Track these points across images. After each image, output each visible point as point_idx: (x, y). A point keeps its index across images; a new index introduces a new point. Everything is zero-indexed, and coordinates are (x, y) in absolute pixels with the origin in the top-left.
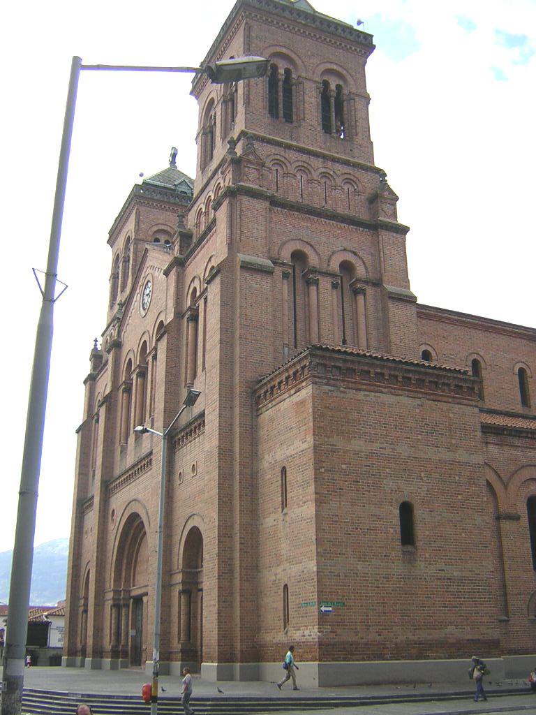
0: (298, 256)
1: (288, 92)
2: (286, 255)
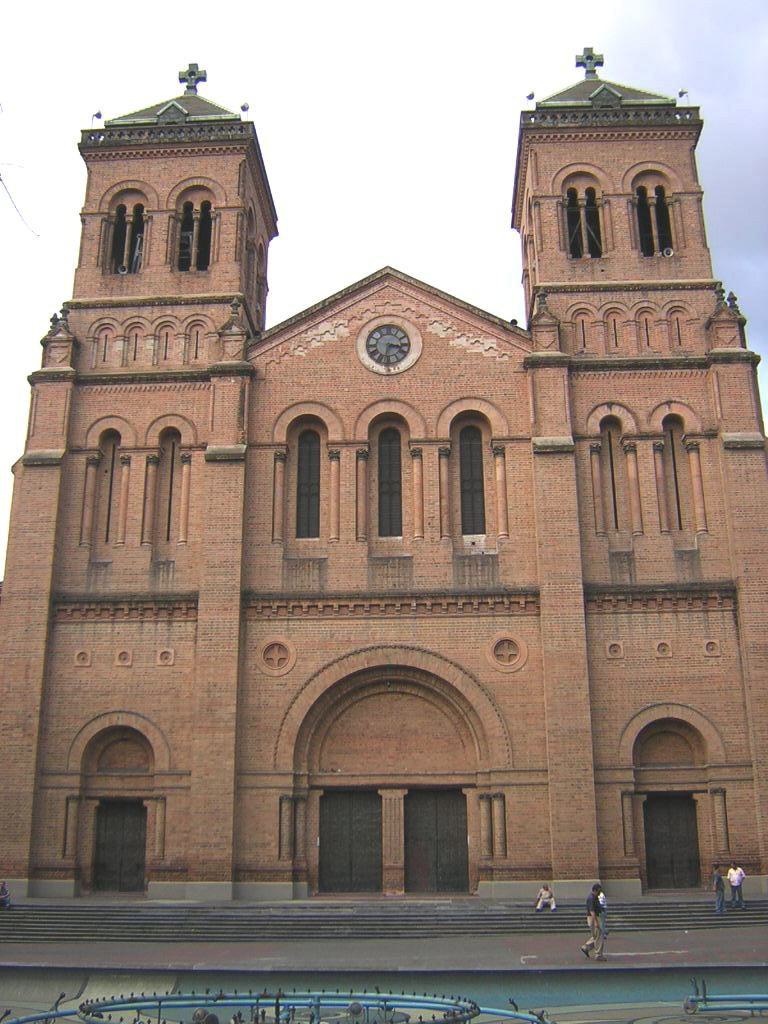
0: (611, 423)
1: (593, 219)
2: (593, 426)
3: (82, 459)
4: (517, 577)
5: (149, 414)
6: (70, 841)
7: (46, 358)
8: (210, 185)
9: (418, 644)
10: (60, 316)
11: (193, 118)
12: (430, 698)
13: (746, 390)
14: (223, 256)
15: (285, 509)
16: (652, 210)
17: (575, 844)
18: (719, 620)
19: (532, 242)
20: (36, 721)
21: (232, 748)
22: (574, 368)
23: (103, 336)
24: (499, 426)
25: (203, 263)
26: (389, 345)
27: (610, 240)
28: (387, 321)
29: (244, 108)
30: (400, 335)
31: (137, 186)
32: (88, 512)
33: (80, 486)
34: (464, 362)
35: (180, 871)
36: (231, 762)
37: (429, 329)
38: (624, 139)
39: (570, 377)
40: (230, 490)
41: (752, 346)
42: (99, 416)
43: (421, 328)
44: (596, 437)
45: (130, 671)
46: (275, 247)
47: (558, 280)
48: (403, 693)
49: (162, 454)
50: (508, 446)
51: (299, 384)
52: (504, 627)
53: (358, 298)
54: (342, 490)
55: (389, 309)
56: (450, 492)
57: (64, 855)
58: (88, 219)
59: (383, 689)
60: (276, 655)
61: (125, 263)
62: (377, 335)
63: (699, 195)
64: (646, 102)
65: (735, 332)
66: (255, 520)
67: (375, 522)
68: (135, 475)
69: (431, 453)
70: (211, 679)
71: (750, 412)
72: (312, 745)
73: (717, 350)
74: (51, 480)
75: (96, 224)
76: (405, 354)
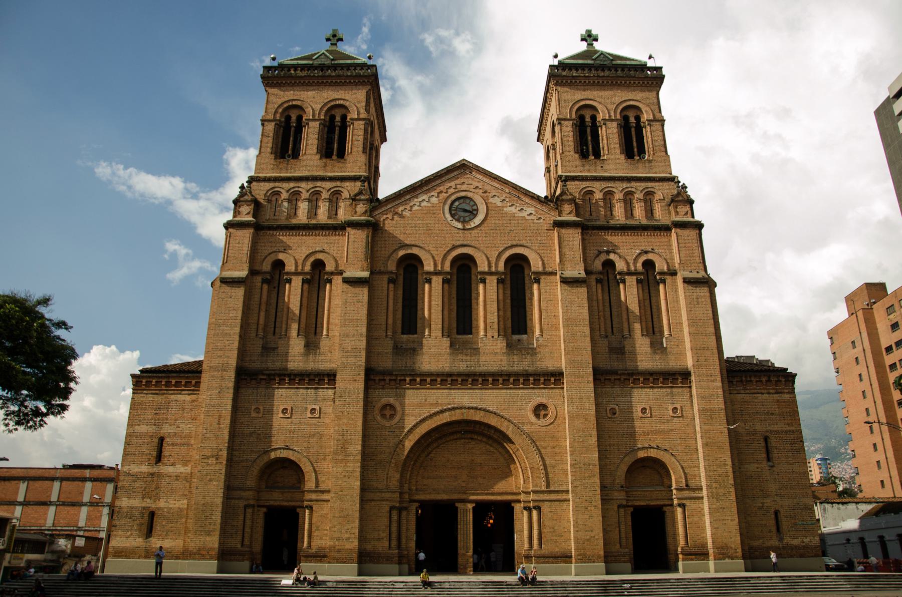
3: (259, 279)
4: (549, 364)
5: (305, 251)
6: (247, 535)
7: (236, 213)
8: (347, 104)
9: (483, 406)
10: (246, 185)
11: (336, 62)
12: (490, 442)
13: (695, 244)
14: (355, 150)
15: (394, 315)
16: (633, 130)
17: (588, 540)
18: (679, 393)
19: (554, 149)
20: (224, 453)
21: (359, 474)
22: (585, 228)
23: (274, 199)
24: (536, 264)
25: (341, 154)
26: (463, 210)
27: (606, 148)
28: (462, 194)
29: (370, 58)
30: (472, 203)
31: (299, 103)
32: (262, 314)
33: (256, 297)
34: (513, 222)
35: (320, 556)
36: (358, 483)
37: (491, 200)
38: (614, 85)
39: (582, 234)
40: (358, 301)
41: (697, 218)
42: (271, 251)
43: (486, 200)
44: (600, 273)
45: (290, 420)
46: (384, 149)
47: (574, 171)
48: (472, 439)
49: (312, 277)
50: (542, 277)
51: (405, 234)
52: (539, 396)
53: (443, 179)
54: (433, 303)
55: (464, 187)
56: (504, 305)
57: (242, 545)
58: (266, 123)
59: (459, 436)
60: (388, 412)
61: (290, 152)
62: (457, 203)
63: (662, 121)
64: (628, 63)
65: (688, 208)
66: (374, 322)
67: (455, 325)
68: (293, 294)
69: (492, 281)
70: (345, 427)
71: (698, 260)
72: (412, 473)
73: (677, 219)
74: (239, 293)
75: (271, 127)
76: (475, 216)
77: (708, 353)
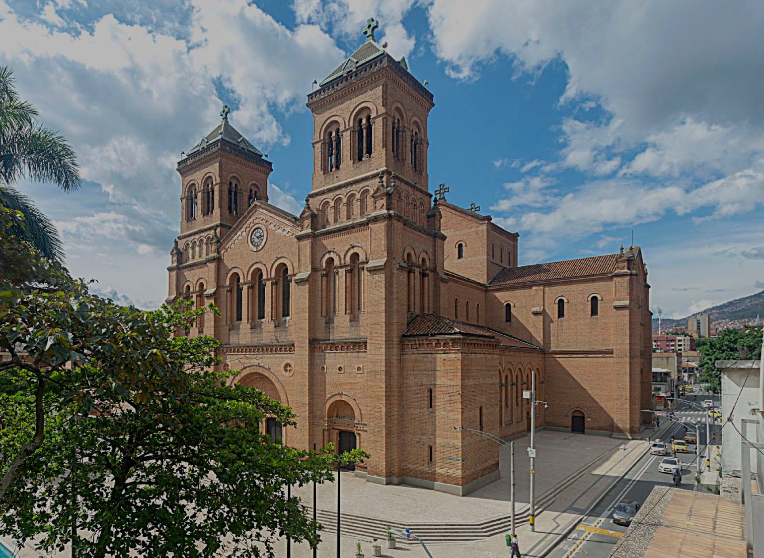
28: (256, 226)
77: (378, 327)
